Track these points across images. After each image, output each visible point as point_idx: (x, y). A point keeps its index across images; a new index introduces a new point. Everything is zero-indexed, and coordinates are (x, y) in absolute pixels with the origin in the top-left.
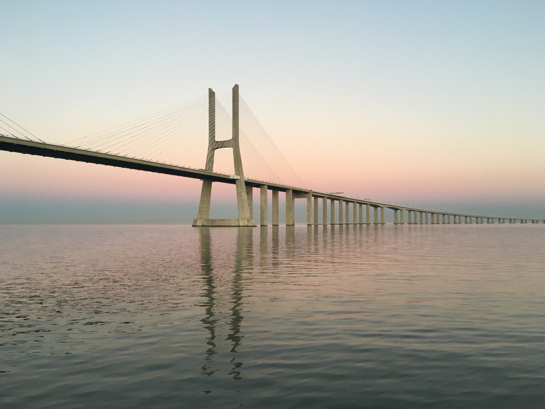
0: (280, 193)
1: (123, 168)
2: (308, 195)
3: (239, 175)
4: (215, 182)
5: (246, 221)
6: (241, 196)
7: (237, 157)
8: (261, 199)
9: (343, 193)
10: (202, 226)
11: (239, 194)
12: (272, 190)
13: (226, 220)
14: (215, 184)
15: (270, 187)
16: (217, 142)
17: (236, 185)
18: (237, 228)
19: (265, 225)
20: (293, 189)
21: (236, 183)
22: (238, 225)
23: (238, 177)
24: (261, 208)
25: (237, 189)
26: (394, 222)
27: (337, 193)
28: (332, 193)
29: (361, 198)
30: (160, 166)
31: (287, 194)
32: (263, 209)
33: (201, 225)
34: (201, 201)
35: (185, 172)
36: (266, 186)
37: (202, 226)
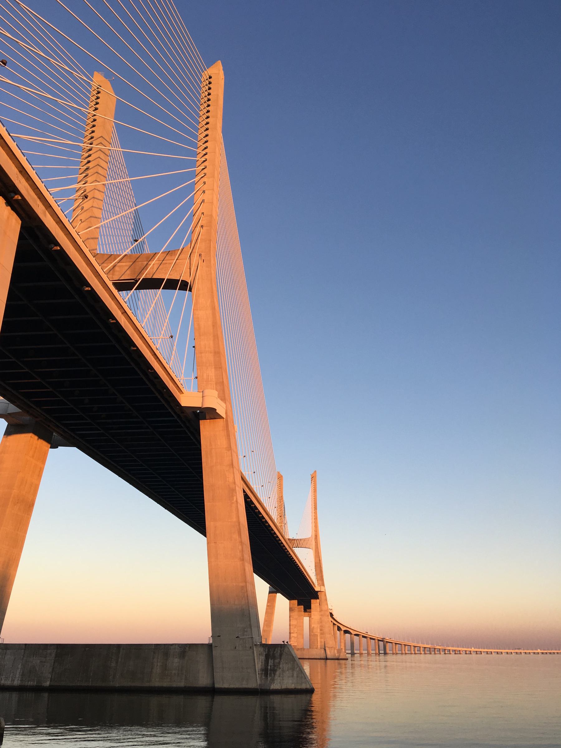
22: (324, 658)
32: (316, 633)
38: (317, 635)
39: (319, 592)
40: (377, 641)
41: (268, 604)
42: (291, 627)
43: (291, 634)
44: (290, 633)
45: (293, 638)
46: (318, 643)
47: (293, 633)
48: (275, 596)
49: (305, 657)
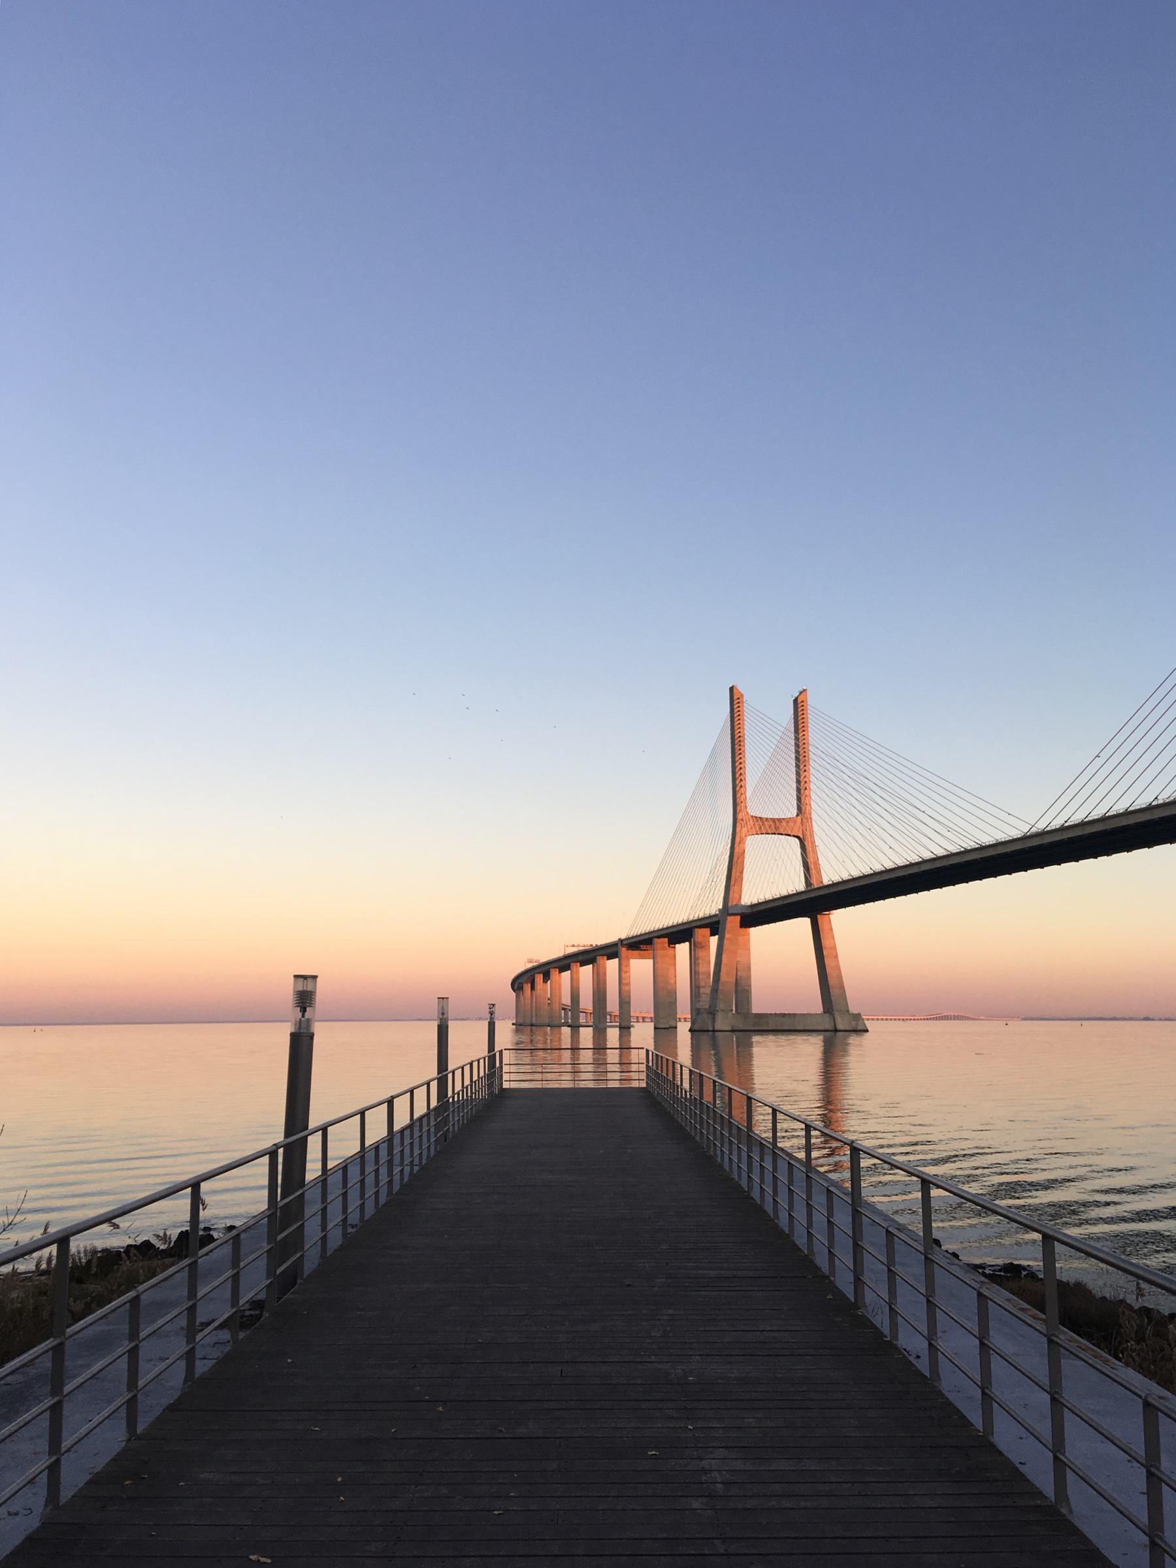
10: (733, 1031)
13: (795, 1014)
22: (830, 1029)
26: (515, 1022)
33: (730, 1029)
37: (733, 1031)
43: (701, 989)
45: (704, 996)
49: (798, 1028)
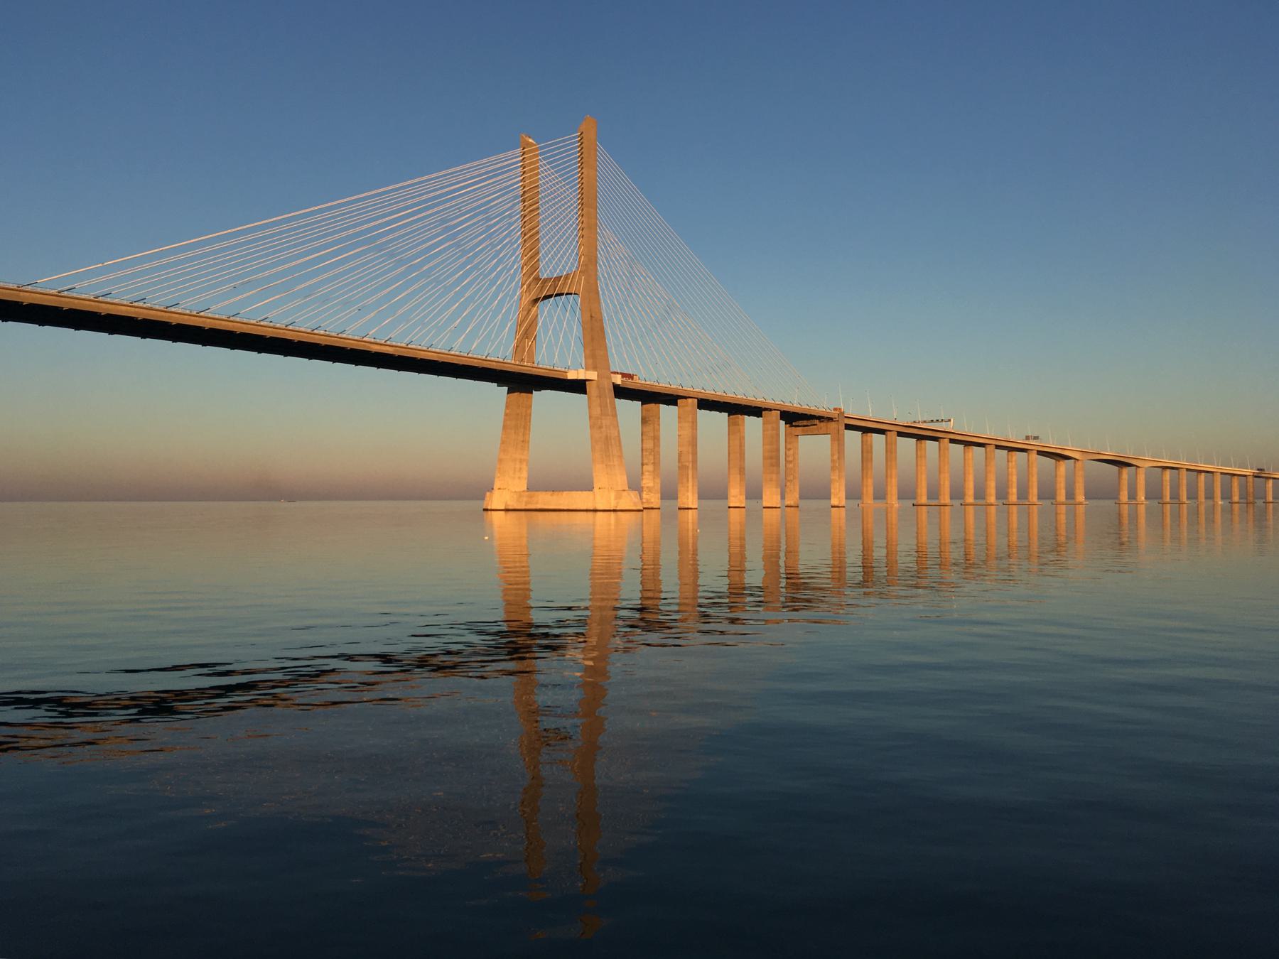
0: (749, 420)
1: (356, 365)
2: (833, 425)
3: (595, 368)
4: (542, 391)
5: (613, 495)
6: (601, 427)
7: (589, 318)
8: (679, 436)
9: (950, 420)
10: (507, 510)
11: (595, 424)
12: (727, 414)
14: (542, 398)
15: (706, 404)
16: (546, 280)
17: (589, 399)
18: (591, 514)
19: (690, 506)
20: (782, 410)
21: (588, 391)
23: (592, 375)
24: (679, 462)
25: (590, 407)
27: (932, 421)
28: (925, 422)
29: (1014, 435)
30: (324, 343)
31: (763, 421)
33: (503, 508)
34: (503, 442)
35: (414, 359)
36: (690, 400)
37: (507, 510)
38: (688, 467)
39: (587, 383)
40: (1250, 479)
41: (508, 411)
42: (644, 453)
44: (643, 465)
45: (647, 473)
46: (688, 481)
47: (647, 464)
48: (532, 397)
